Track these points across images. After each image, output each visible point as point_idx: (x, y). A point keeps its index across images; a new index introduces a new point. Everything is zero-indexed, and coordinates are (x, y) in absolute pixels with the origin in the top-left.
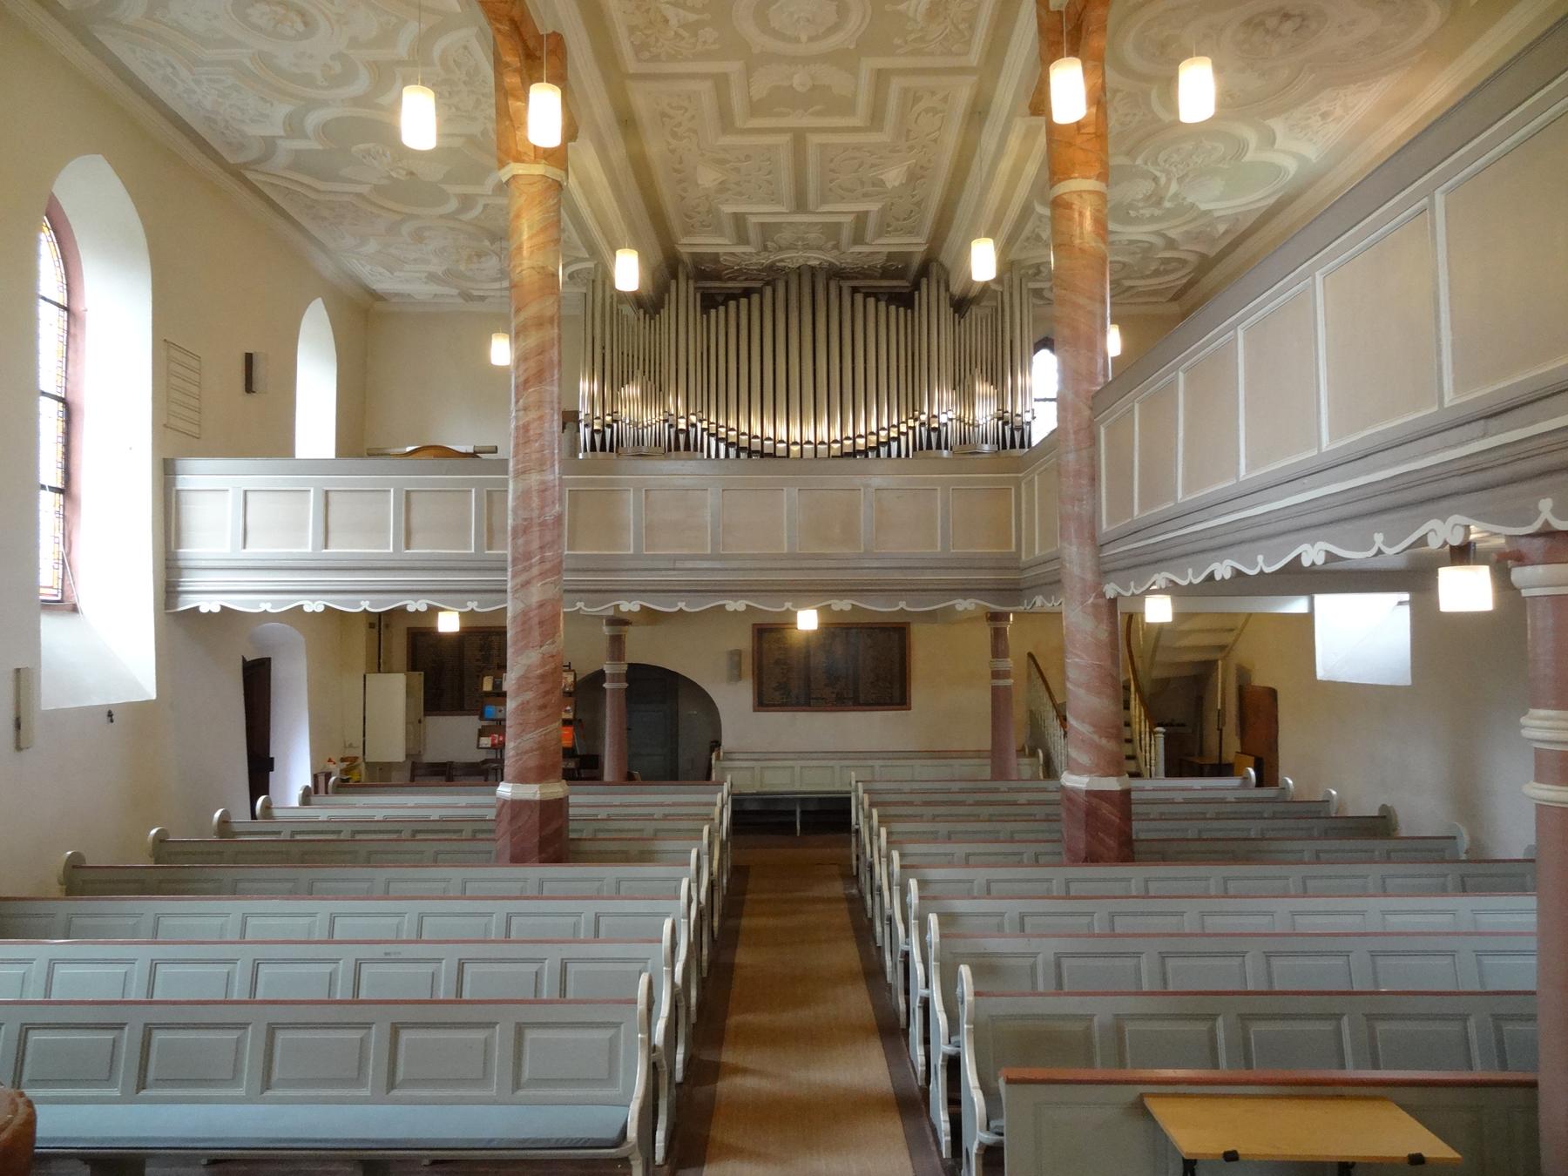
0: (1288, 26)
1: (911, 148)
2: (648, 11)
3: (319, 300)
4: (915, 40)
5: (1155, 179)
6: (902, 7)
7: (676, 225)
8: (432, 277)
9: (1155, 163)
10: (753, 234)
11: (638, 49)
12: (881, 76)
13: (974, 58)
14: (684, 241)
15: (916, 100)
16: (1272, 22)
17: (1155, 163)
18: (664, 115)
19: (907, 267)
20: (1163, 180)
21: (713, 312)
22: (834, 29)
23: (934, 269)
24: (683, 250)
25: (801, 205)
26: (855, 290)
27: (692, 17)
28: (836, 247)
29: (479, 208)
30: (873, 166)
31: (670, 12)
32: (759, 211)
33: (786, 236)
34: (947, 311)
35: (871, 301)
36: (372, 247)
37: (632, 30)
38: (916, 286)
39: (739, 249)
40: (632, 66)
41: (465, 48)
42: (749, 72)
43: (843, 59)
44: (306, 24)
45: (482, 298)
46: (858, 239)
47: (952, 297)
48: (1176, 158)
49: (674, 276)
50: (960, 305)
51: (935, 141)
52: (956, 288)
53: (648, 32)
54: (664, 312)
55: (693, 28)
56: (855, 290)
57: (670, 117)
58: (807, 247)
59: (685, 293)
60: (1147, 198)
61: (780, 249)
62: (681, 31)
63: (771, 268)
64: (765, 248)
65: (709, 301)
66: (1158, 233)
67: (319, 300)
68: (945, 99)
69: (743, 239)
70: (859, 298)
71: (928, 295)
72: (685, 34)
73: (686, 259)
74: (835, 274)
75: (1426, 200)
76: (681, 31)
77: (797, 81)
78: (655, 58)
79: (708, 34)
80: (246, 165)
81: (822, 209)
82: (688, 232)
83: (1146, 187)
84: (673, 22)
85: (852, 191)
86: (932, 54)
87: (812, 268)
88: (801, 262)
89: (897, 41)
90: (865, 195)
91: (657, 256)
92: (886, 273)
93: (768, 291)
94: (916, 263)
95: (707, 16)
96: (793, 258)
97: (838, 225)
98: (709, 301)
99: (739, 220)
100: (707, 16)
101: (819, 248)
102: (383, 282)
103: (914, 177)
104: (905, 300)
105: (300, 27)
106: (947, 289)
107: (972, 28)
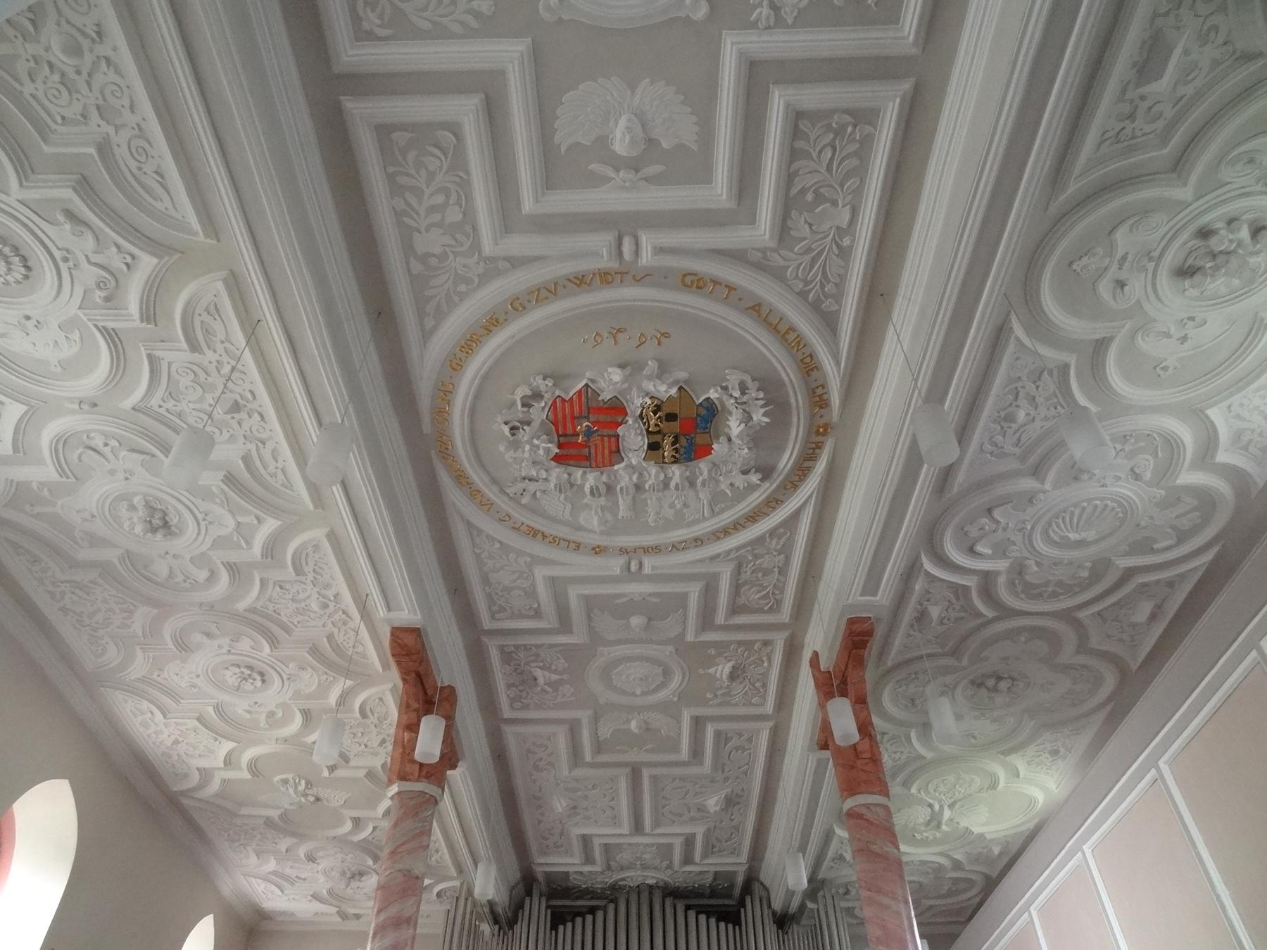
0: (1003, 685)
1: (727, 779)
2: (522, 673)
3: (211, 916)
4: (723, 695)
5: (930, 806)
6: (712, 670)
7: (534, 847)
8: (315, 897)
9: (927, 792)
10: (598, 854)
11: (512, 701)
13: (769, 708)
14: (542, 860)
15: (727, 740)
16: (991, 683)
17: (927, 792)
18: (528, 751)
19: (732, 886)
20: (937, 807)
21: (561, 928)
22: (663, 685)
23: (757, 888)
24: (539, 871)
25: (638, 827)
26: (688, 908)
27: (554, 677)
28: (670, 867)
29: (370, 829)
30: (696, 794)
31: (539, 673)
32: (602, 832)
33: (625, 857)
34: (771, 928)
35: (703, 918)
36: (272, 865)
37: (509, 686)
38: (742, 903)
39: (586, 869)
40: (507, 713)
41: (381, 699)
42: (596, 719)
44: (263, 681)
45: (358, 917)
46: (688, 860)
47: (774, 913)
48: (942, 788)
49: (529, 893)
50: (783, 921)
51: (746, 773)
52: (777, 905)
54: (517, 928)
55: (555, 685)
56: (688, 908)
57: (534, 753)
58: (645, 867)
59: (538, 909)
60: (928, 823)
61: (622, 869)
62: (547, 688)
63: (615, 888)
64: (609, 868)
65: (558, 919)
66: (941, 854)
67: (211, 916)
68: (750, 740)
69: (589, 860)
70: (692, 914)
71: (752, 913)
73: (540, 877)
74: (672, 893)
75: (1153, 771)
76: (547, 688)
77: (633, 725)
78: (526, 707)
79: (567, 689)
80: (183, 793)
81: (658, 831)
82: (544, 853)
83: (922, 814)
84: (541, 681)
85: (681, 815)
86: (736, 705)
87: (651, 887)
88: (640, 881)
90: (692, 819)
91: (515, 875)
92: (714, 892)
93: (611, 907)
94: (740, 880)
95: (565, 677)
96: (634, 877)
97: (670, 847)
98: (558, 919)
99: (586, 840)
100: (565, 677)
101: (656, 868)
102: (272, 898)
103: (731, 802)
104: (731, 916)
105: (259, 683)
106: (770, 906)
107: (764, 685)
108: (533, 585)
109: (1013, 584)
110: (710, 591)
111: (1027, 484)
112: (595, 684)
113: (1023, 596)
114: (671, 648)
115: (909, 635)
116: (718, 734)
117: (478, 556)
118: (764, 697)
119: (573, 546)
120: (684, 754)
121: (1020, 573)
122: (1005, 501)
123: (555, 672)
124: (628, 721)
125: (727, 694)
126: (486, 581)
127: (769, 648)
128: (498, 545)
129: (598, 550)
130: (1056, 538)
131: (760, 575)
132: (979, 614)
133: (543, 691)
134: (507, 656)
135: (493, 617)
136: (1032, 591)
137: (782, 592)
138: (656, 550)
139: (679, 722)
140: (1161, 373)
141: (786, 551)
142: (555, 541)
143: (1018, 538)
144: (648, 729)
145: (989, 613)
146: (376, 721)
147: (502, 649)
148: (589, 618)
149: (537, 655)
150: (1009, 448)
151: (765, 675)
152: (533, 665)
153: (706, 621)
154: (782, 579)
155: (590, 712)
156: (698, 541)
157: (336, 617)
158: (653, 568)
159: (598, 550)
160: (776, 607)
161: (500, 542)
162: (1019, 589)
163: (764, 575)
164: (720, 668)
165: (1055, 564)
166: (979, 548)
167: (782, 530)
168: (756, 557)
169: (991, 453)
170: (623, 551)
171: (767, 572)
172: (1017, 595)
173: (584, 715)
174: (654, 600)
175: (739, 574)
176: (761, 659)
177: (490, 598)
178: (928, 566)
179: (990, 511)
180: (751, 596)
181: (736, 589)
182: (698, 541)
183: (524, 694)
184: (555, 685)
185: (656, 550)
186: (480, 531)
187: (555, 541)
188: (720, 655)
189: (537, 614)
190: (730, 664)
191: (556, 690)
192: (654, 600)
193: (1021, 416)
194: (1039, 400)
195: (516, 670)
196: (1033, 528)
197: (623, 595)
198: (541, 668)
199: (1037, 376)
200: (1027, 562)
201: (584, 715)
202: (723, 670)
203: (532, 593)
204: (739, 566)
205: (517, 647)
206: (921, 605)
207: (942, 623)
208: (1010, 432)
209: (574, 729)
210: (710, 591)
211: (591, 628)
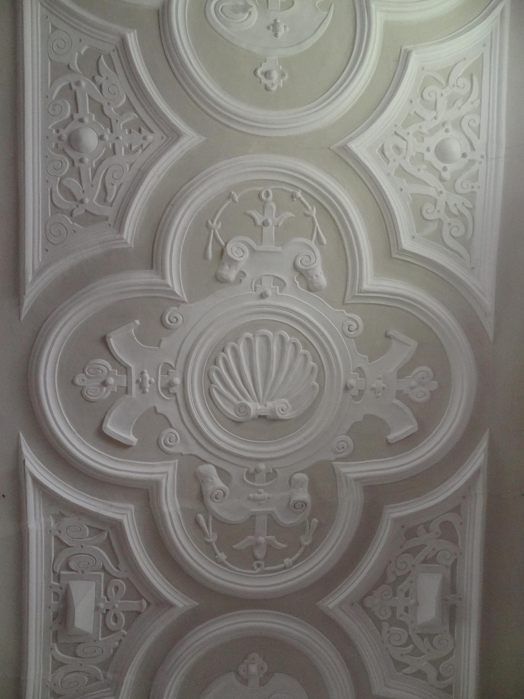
109: (197, 522)
111: (142, 278)
113: (222, 556)
115: (58, 665)
121: (201, 497)
122: (118, 314)
130: (231, 412)
132: (164, 604)
136: (230, 539)
140: (264, 81)
143: (169, 409)
145: (180, 601)
150: (91, 201)
162: (212, 537)
165: (251, 476)
166: (111, 428)
169: (71, 215)
172: (208, 549)
178: (34, 466)
179: (104, 341)
193: (90, 139)
194: (111, 111)
196: (184, 382)
199: (92, 65)
200: (203, 468)
206: (58, 578)
207: (107, 631)
208: (87, 172)
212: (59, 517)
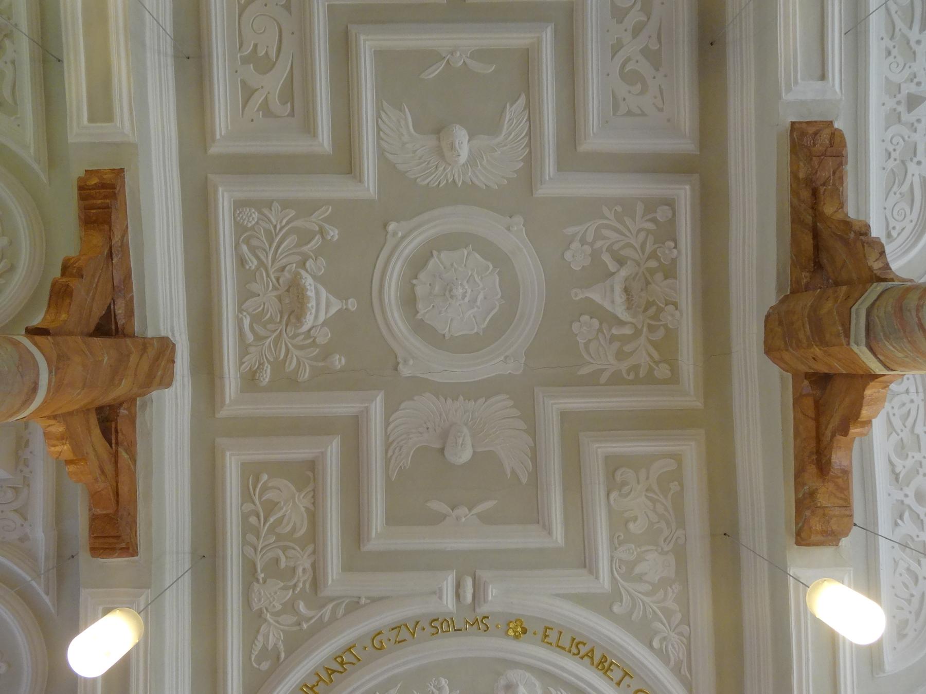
12: (346, 161)
22: (418, 263)
31: (621, 311)
37: (670, 272)
42: (529, 174)
43: (406, 196)
53: (653, 264)
55: (597, 274)
62: (612, 266)
68: (249, 93)
72: (606, 258)
76: (612, 266)
78: (651, 205)
84: (619, 298)
86: (286, 204)
89: (334, 233)
95: (579, 295)
107: (241, 261)
108: (613, 548)
110: (356, 529)
112: (529, 266)
114: (405, 371)
116: (309, 127)
117: (686, 620)
118: (240, 229)
119: (553, 636)
120: (368, 44)
123: (595, 310)
124: (473, 159)
125: (305, 237)
126: (681, 555)
127: (245, 367)
128: (656, 644)
129: (520, 629)
131: (283, 564)
133: (621, 262)
134: (666, 347)
135: (677, 458)
137: (245, 517)
138: (439, 625)
139: (381, 153)
141: (254, 620)
142: (579, 647)
144: (439, 130)
146: (912, 167)
147: (674, 378)
148: (534, 458)
149: (620, 355)
151: (245, 294)
152: (627, 331)
153: (353, 431)
154: (249, 550)
155: (542, 192)
156: (378, 643)
157: (909, 463)
158: (438, 593)
159: (520, 629)
160: (252, 473)
161: (651, 646)
163: (277, 561)
164: (322, 318)
167: (265, 666)
168: (290, 607)
170: (481, 624)
171: (274, 569)
173: (554, 185)
174: (437, 506)
175: (314, 566)
176: (259, 338)
177: (681, 522)
180: (293, 510)
181: (314, 536)
182: (378, 643)
183: (649, 248)
184: (597, 274)
185: (439, 625)
186: (676, 671)
187: (579, 647)
188: (326, 353)
189: (613, 464)
190: (305, 328)
191: (595, 255)
192: (437, 506)
195: (656, 317)
197: (487, 519)
198: (622, 323)
201: (554, 185)
202: (321, 306)
203: (619, 522)
204: (316, 584)
205: (650, 379)
209: (572, 156)
210: (356, 529)
211: (532, 430)
212: (24, 539)
